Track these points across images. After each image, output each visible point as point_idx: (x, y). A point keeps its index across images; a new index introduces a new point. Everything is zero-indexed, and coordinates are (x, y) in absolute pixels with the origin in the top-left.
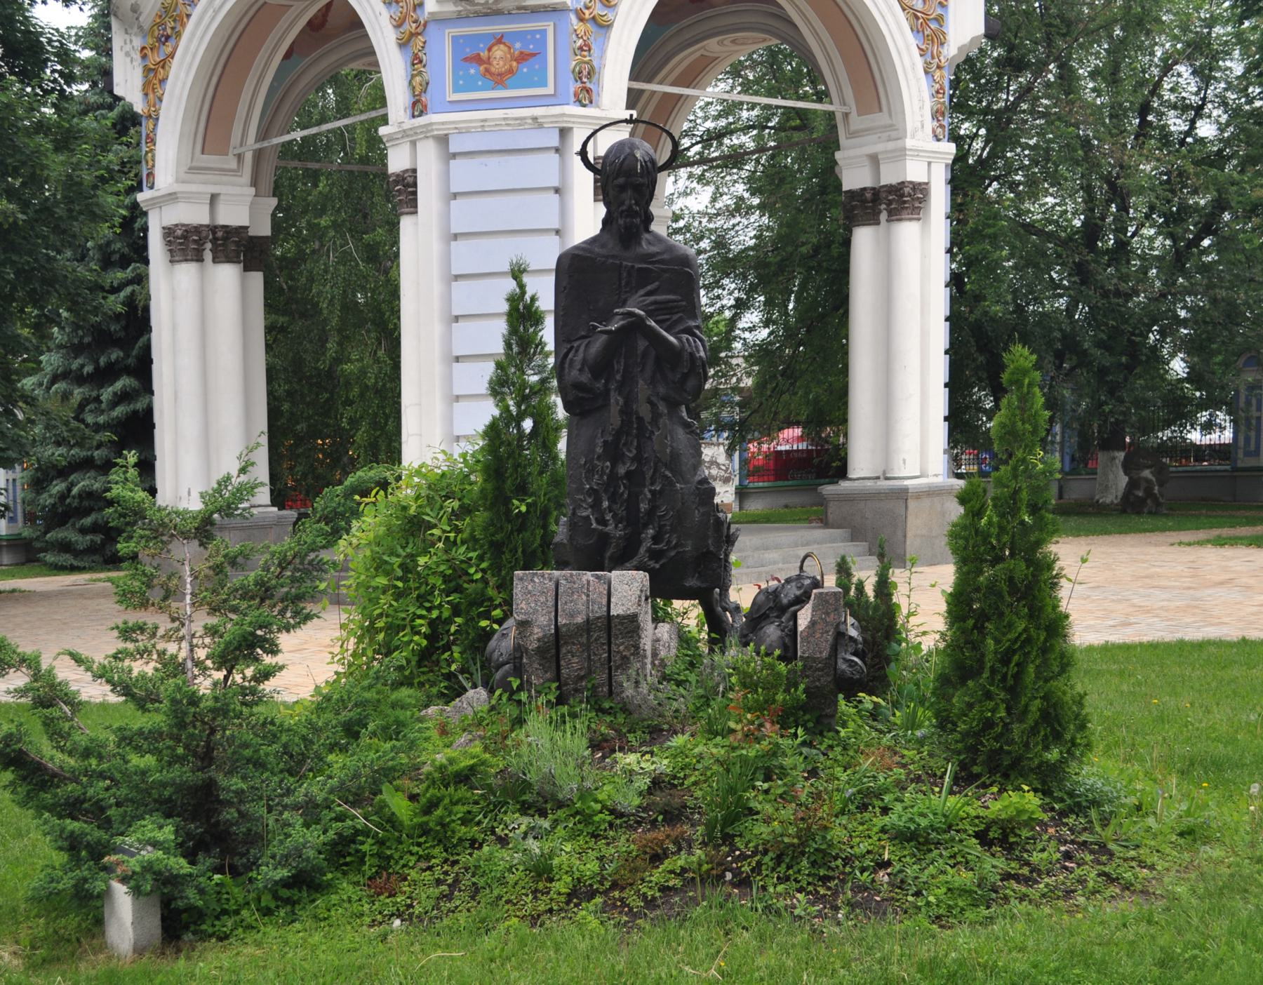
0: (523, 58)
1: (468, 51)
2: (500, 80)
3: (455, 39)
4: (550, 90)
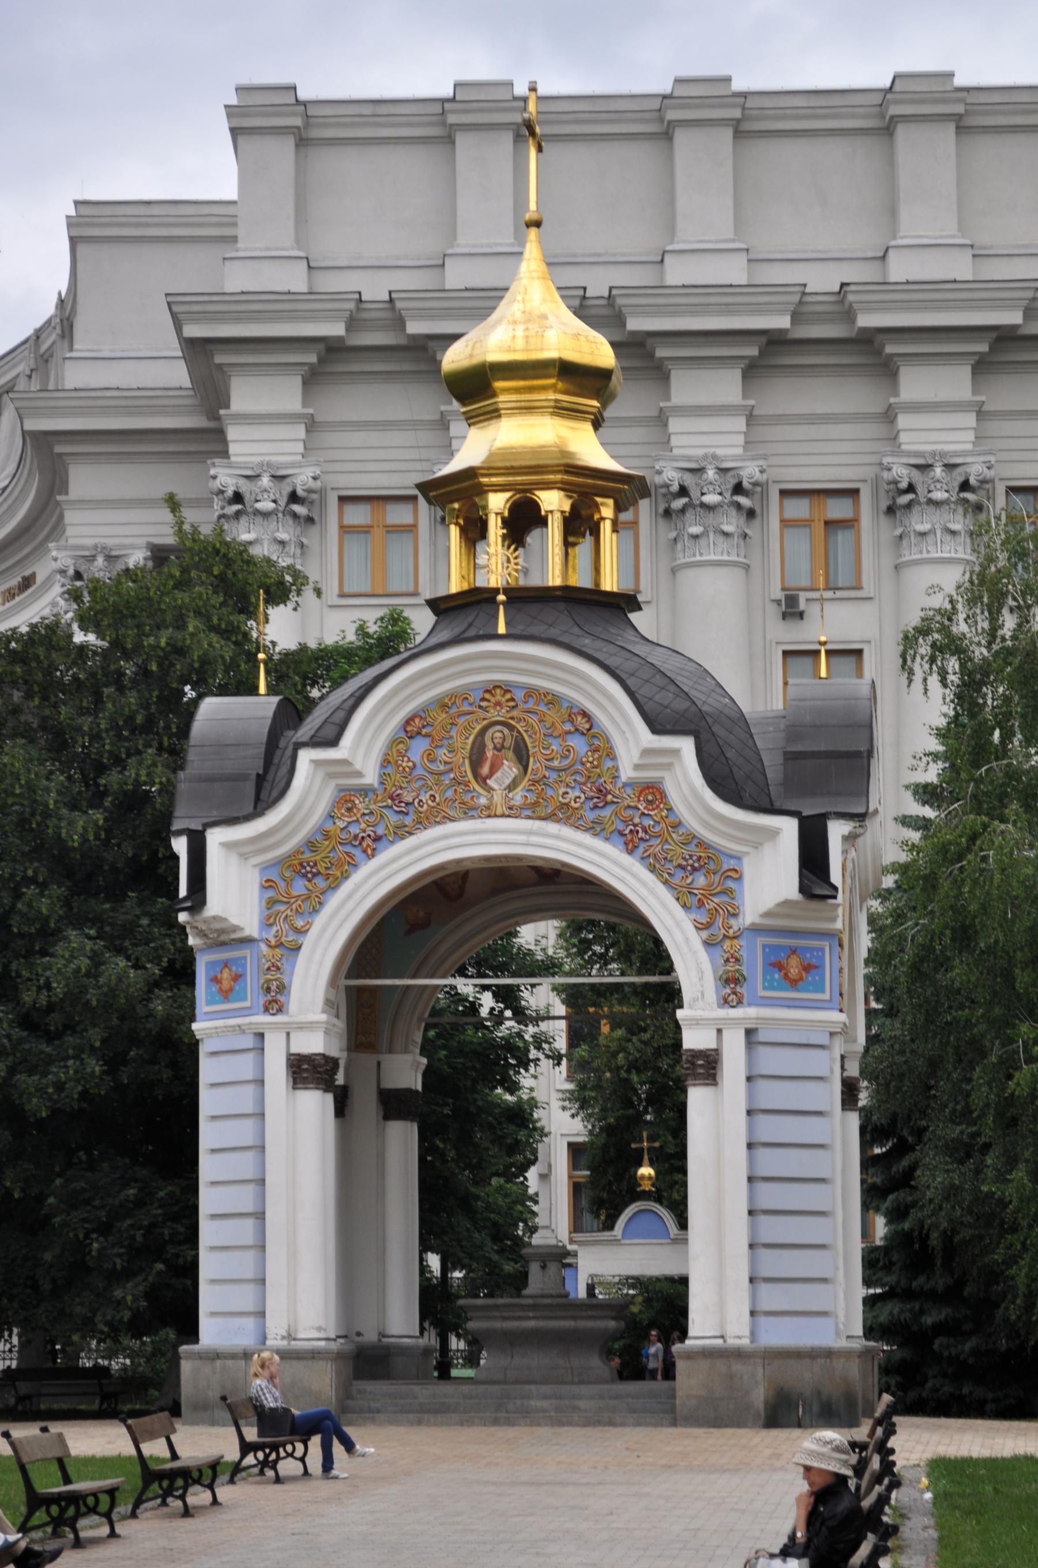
0: (808, 968)
1: (773, 959)
2: (794, 983)
3: (764, 946)
4: (826, 996)
